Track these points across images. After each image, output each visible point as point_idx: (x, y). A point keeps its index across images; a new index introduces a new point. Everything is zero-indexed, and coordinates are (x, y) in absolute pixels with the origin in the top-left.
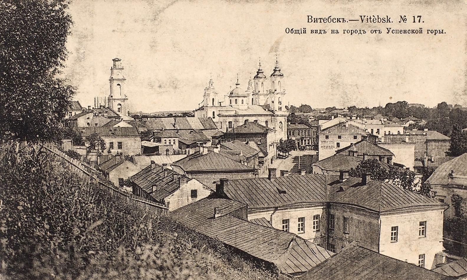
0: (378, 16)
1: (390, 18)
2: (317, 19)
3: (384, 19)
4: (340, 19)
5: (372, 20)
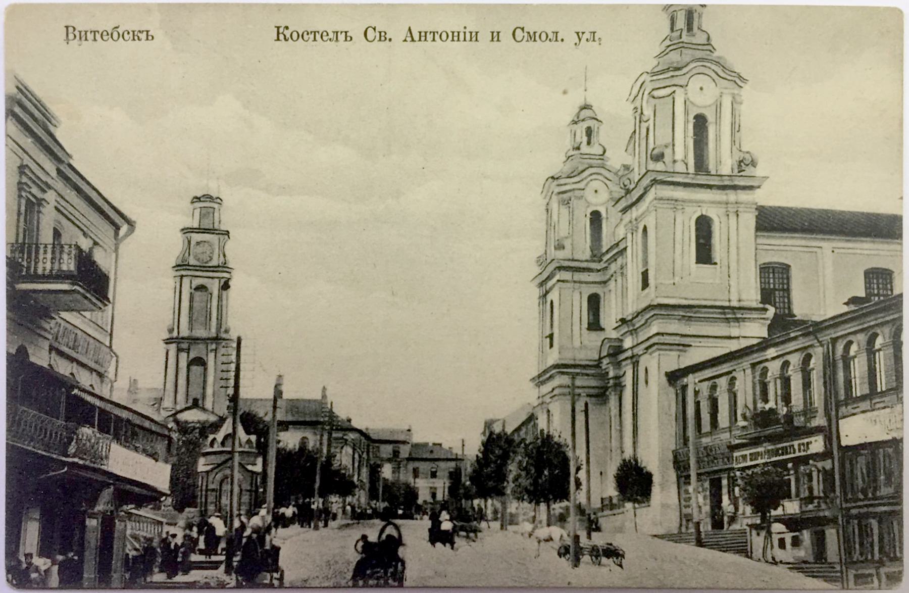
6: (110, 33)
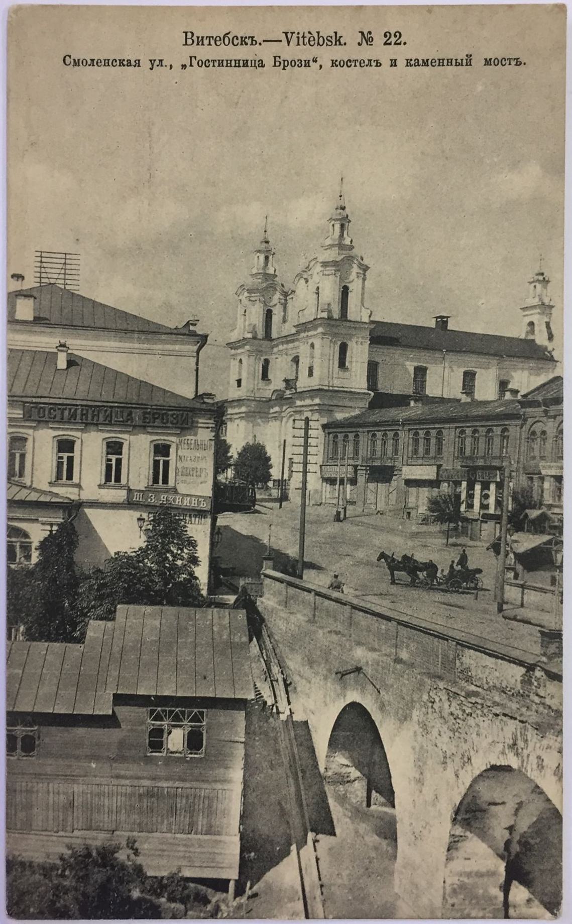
0: (318, 33)
1: (340, 37)
2: (203, 37)
3: (329, 38)
4: (246, 38)
5: (306, 40)
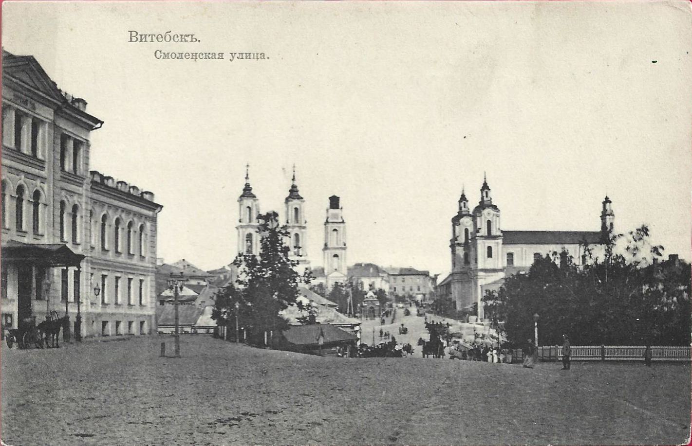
4: (186, 36)
6: (163, 37)
